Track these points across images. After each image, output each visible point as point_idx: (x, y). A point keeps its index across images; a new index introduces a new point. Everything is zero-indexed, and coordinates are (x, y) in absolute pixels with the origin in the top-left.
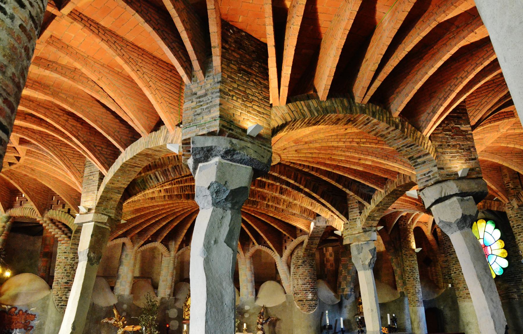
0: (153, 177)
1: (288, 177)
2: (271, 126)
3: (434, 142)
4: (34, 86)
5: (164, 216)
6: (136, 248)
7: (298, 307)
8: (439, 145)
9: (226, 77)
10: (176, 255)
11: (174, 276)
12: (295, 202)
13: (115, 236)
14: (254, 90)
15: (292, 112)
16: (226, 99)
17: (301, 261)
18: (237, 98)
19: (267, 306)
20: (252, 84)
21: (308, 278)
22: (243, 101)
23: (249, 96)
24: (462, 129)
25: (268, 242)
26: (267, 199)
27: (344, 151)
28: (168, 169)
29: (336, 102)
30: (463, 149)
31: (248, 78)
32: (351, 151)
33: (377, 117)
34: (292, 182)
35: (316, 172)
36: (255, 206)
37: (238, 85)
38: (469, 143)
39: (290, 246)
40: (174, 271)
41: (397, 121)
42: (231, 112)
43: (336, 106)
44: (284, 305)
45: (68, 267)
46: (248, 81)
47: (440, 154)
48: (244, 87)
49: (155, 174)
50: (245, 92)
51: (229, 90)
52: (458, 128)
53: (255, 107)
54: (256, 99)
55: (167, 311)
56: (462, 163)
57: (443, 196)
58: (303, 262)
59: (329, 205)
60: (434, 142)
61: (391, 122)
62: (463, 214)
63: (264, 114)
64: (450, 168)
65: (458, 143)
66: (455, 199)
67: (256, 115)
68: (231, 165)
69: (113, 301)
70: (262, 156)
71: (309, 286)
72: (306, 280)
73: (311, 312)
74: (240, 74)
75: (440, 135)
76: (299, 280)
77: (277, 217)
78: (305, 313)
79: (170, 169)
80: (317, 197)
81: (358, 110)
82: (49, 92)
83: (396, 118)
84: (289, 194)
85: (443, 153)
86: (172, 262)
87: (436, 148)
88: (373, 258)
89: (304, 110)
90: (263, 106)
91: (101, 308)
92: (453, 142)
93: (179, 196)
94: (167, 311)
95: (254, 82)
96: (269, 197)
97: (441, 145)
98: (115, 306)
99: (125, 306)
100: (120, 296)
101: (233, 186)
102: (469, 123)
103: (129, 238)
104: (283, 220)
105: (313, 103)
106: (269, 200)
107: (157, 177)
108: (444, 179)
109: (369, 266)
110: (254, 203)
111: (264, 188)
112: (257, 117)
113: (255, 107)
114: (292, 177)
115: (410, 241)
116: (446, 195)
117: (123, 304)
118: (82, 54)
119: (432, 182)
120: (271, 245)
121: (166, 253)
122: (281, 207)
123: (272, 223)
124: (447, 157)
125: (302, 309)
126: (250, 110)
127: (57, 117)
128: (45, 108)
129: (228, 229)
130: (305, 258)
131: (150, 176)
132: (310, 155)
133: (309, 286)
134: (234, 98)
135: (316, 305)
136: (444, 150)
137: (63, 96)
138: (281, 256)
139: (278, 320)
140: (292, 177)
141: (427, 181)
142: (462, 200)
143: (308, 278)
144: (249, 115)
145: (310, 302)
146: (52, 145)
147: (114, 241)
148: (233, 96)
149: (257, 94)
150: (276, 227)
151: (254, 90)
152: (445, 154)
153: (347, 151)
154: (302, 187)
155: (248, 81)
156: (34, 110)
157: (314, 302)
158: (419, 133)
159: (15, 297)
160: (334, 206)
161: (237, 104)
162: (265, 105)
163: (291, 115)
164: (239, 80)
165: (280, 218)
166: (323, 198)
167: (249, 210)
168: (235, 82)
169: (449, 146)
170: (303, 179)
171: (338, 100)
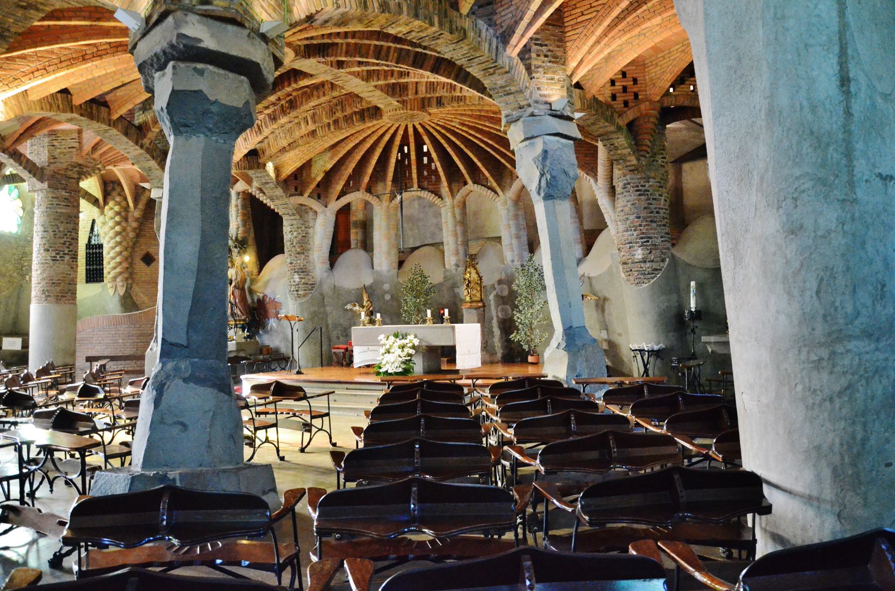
1: (362, 57)
6: (385, 203)
10: (455, 202)
11: (459, 236)
19: (591, 275)
21: (632, 217)
35: (353, 37)
40: (458, 228)
55: (457, 290)
69: (368, 281)
71: (635, 233)
72: (628, 222)
73: (645, 285)
76: (619, 223)
86: (449, 214)
88: (542, 175)
91: (349, 292)
93: (348, 119)
100: (379, 273)
103: (362, 191)
109: (539, 194)
114: (371, 52)
117: (383, 283)
121: (437, 201)
130: (628, 177)
133: (635, 233)
135: (656, 270)
138: (596, 180)
139: (605, 299)
143: (632, 217)
145: (639, 265)
147: (342, 199)
157: (648, 265)
159: (267, 283)
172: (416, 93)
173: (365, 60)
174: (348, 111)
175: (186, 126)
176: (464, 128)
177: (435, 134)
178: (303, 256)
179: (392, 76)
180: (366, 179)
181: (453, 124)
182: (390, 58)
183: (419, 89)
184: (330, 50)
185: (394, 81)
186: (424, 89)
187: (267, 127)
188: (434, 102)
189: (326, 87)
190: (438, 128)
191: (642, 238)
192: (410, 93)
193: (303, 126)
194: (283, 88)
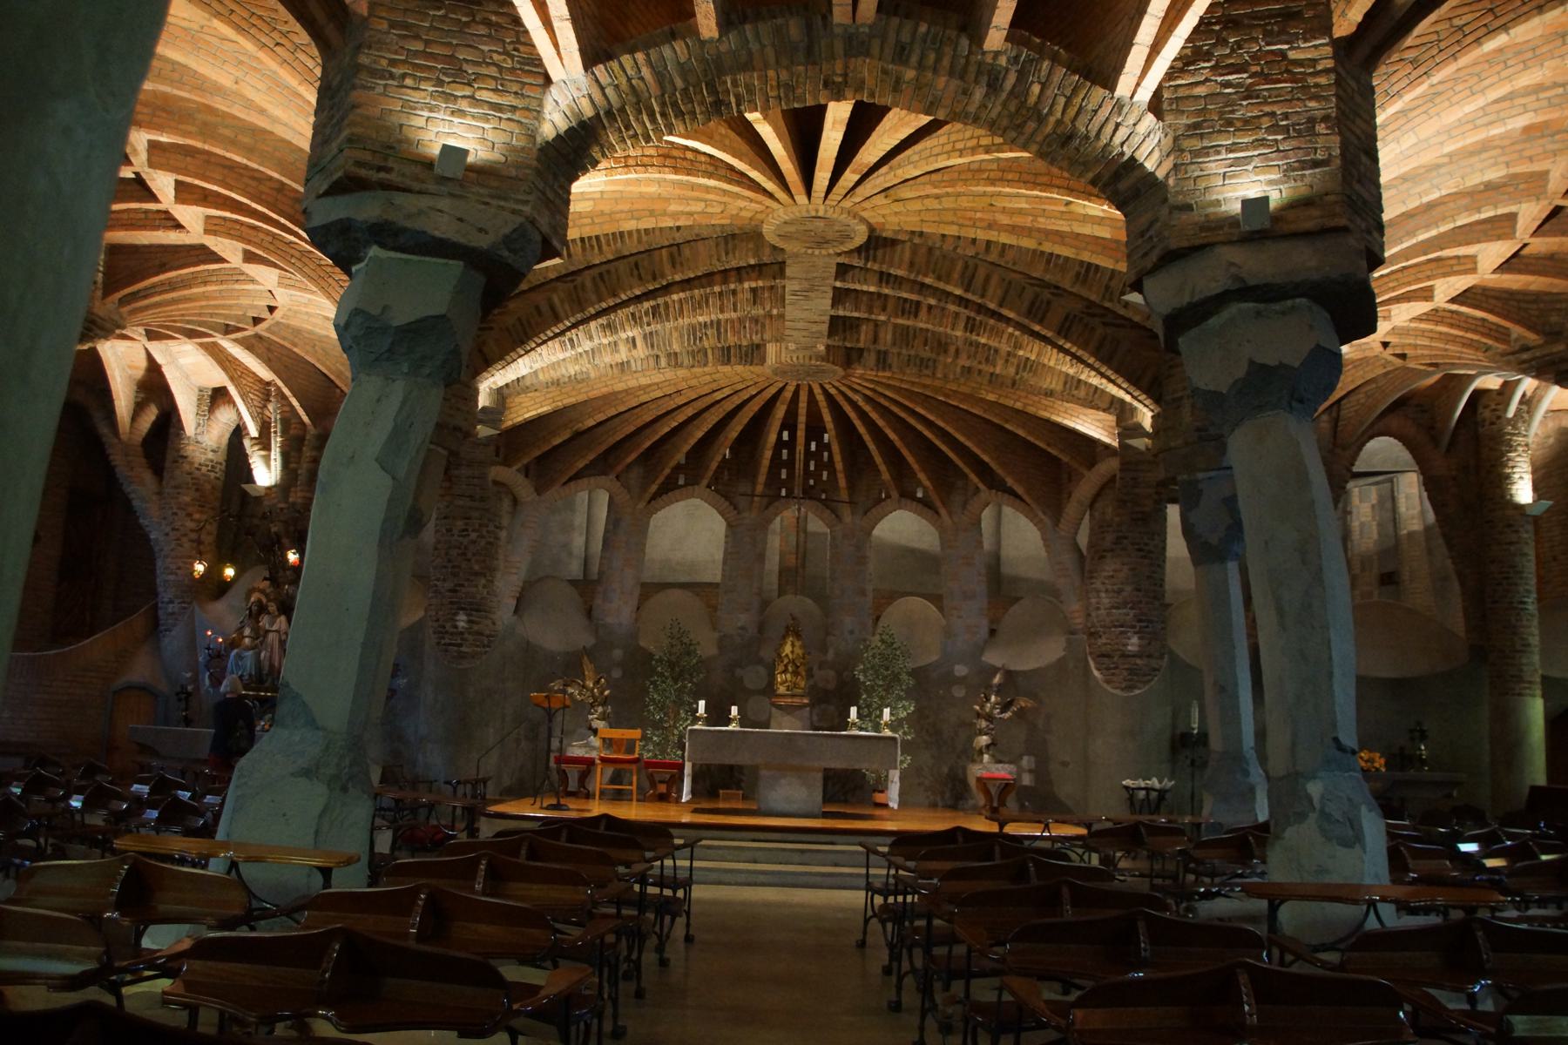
0: (545, 308)
1: (939, 278)
2: (539, 140)
3: (1169, 119)
4: (156, 120)
5: (689, 412)
7: (1096, 673)
8: (1189, 127)
9: (385, 26)
12: (1021, 353)
13: (572, 473)
14: (486, 48)
15: (602, 89)
16: (380, 90)
17: (1110, 538)
18: (414, 77)
20: (483, 30)
22: (440, 83)
23: (465, 67)
24: (1292, 55)
25: (1010, 482)
26: (952, 349)
27: (992, 182)
28: (583, 285)
29: (757, 36)
30: (1286, 129)
31: (466, 15)
32: (1010, 176)
33: (914, 59)
34: (958, 292)
36: (926, 372)
37: (427, 43)
38: (1312, 104)
39: (1085, 488)
41: (1003, 61)
42: (394, 119)
43: (754, 47)
44: (1060, 664)
45: (454, 552)
46: (467, 24)
47: (1187, 158)
48: (449, 44)
49: (550, 300)
50: (451, 58)
51: (393, 63)
52: (1283, 54)
53: (484, 95)
54: (493, 71)
56: (1271, 182)
57: (1186, 299)
58: (1118, 541)
59: (1091, 361)
60: (1169, 119)
61: (972, 69)
62: (1252, 362)
63: (514, 108)
64: (1218, 203)
65: (1267, 109)
66: (1234, 309)
67: (485, 118)
68: (407, 261)
70: (481, 230)
71: (1132, 613)
74: (439, 9)
75: (1201, 91)
77: (1010, 403)
78: (1118, 692)
79: (589, 284)
80: (1049, 334)
81: (839, 47)
82: (193, 129)
83: (997, 54)
84: (999, 334)
85: (1205, 151)
87: (1176, 139)
89: (642, 79)
90: (515, 88)
92: (1244, 110)
93: (699, 356)
94: (739, 672)
95: (489, 24)
96: (960, 343)
97: (1196, 126)
98: (587, 652)
99: (618, 653)
101: (400, 318)
102: (1327, 29)
103: (612, 476)
104: (1031, 410)
105: (676, 52)
106: (957, 351)
107: (553, 308)
108: (1185, 244)
110: (923, 363)
111: (916, 316)
112: (487, 121)
113: (484, 95)
114: (956, 276)
115: (1508, 477)
116: (1196, 299)
118: (185, 24)
119: (1154, 257)
120: (1020, 490)
122: (998, 371)
123: (1007, 421)
124: (1214, 166)
125: (1108, 682)
126: (464, 105)
127: (254, 183)
128: (225, 167)
129: (390, 426)
131: (537, 308)
132: (935, 204)
133: (1132, 613)
134: (409, 82)
136: (1206, 143)
137: (227, 132)
140: (956, 276)
141: (1146, 254)
142: (1258, 314)
143: (1129, 588)
144: (456, 120)
146: (297, 254)
148: (404, 76)
149: (496, 57)
150: (1021, 432)
151: (486, 48)
152: (1208, 155)
153: (1001, 180)
154: (992, 306)
155: (467, 24)
156: (196, 177)
158: (1099, 93)
160: (1107, 361)
161: (415, 96)
162: (524, 84)
163: (597, 96)
164: (432, 28)
165: (1019, 405)
166: (1066, 338)
167: (925, 386)
168: (417, 37)
169: (1230, 123)
170: (994, 281)
171: (765, 28)
172: (875, 340)
173: (941, 285)
174: (732, 340)
175: (1301, 401)
176: (867, 408)
177: (847, 408)
178: (483, 581)
179: (884, 309)
180: (633, 456)
181: (856, 397)
182: (990, 292)
183: (881, 335)
184: (880, 253)
185: (882, 318)
186: (889, 337)
187: (591, 338)
188: (871, 359)
189: (740, 296)
190: (820, 398)
191: (1140, 621)
192: (862, 337)
193: (623, 348)
194: (711, 284)
